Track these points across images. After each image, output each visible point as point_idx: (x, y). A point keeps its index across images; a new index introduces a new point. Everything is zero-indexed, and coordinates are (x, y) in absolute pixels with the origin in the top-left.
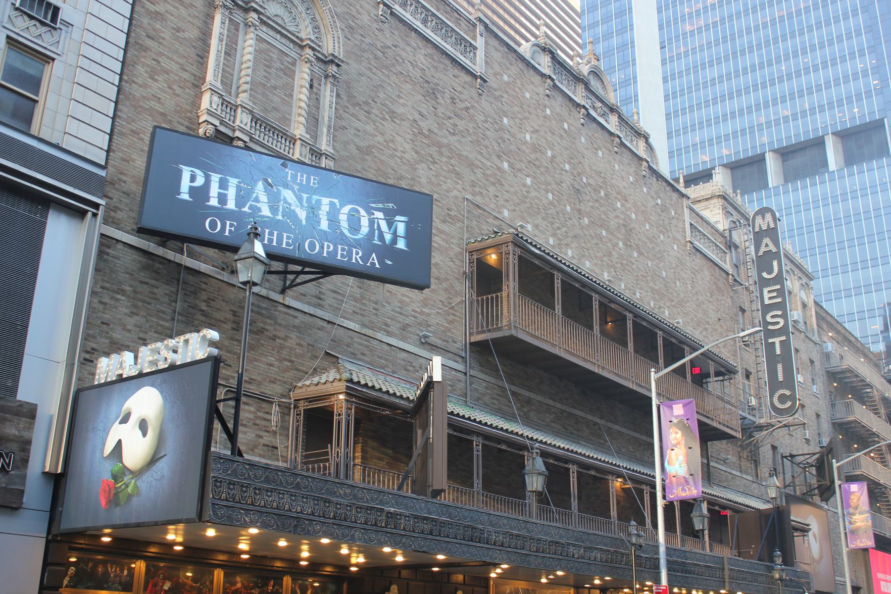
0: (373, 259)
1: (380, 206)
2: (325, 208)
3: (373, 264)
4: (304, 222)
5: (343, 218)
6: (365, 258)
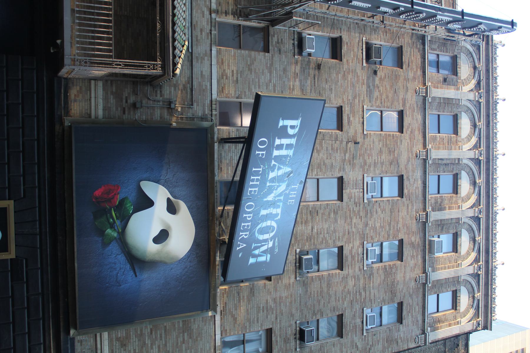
0: (242, 245)
2: (274, 211)
3: (239, 246)
4: (265, 200)
5: (269, 223)
6: (243, 241)
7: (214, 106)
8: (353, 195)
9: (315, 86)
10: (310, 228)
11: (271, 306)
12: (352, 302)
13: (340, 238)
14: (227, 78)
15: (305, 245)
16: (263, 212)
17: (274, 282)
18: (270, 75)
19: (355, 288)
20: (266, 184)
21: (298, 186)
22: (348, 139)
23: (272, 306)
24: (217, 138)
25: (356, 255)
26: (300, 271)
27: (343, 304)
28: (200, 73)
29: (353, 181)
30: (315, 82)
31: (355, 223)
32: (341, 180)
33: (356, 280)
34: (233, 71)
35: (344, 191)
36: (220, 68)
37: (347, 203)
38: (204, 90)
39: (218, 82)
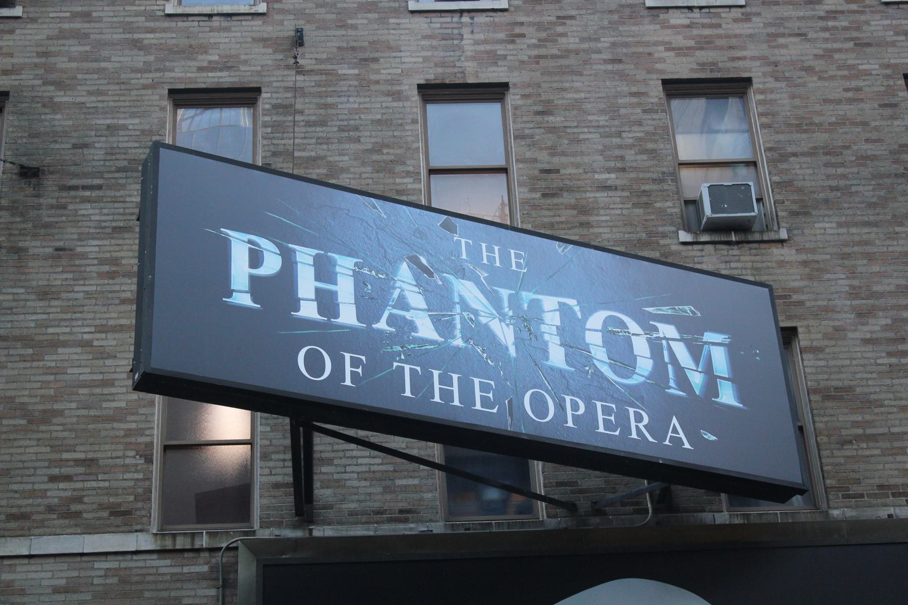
0: (675, 431)
1: (666, 310)
2: (552, 319)
3: (677, 441)
4: (512, 351)
5: (594, 339)
6: (658, 427)
7: (181, 543)
8: (481, 48)
9: (99, 187)
10: (602, 197)
11: (886, 328)
12: (861, 45)
13: (634, 89)
14: (79, 500)
15: (662, 211)
16: (557, 357)
17: (800, 318)
18: (65, 344)
19: (811, 35)
20: (458, 349)
21: (463, 240)
22: (288, 67)
23: (883, 322)
24: (295, 527)
25: (695, 32)
26: (756, 227)
27: (868, 73)
28: (61, 597)
29: (434, 48)
30: (84, 188)
31: (583, 40)
32: (433, 92)
33: (782, 30)
34: (53, 479)
35: (471, 80)
36: (41, 524)
37: (511, 69)
38: (123, 581)
39: (91, 529)
